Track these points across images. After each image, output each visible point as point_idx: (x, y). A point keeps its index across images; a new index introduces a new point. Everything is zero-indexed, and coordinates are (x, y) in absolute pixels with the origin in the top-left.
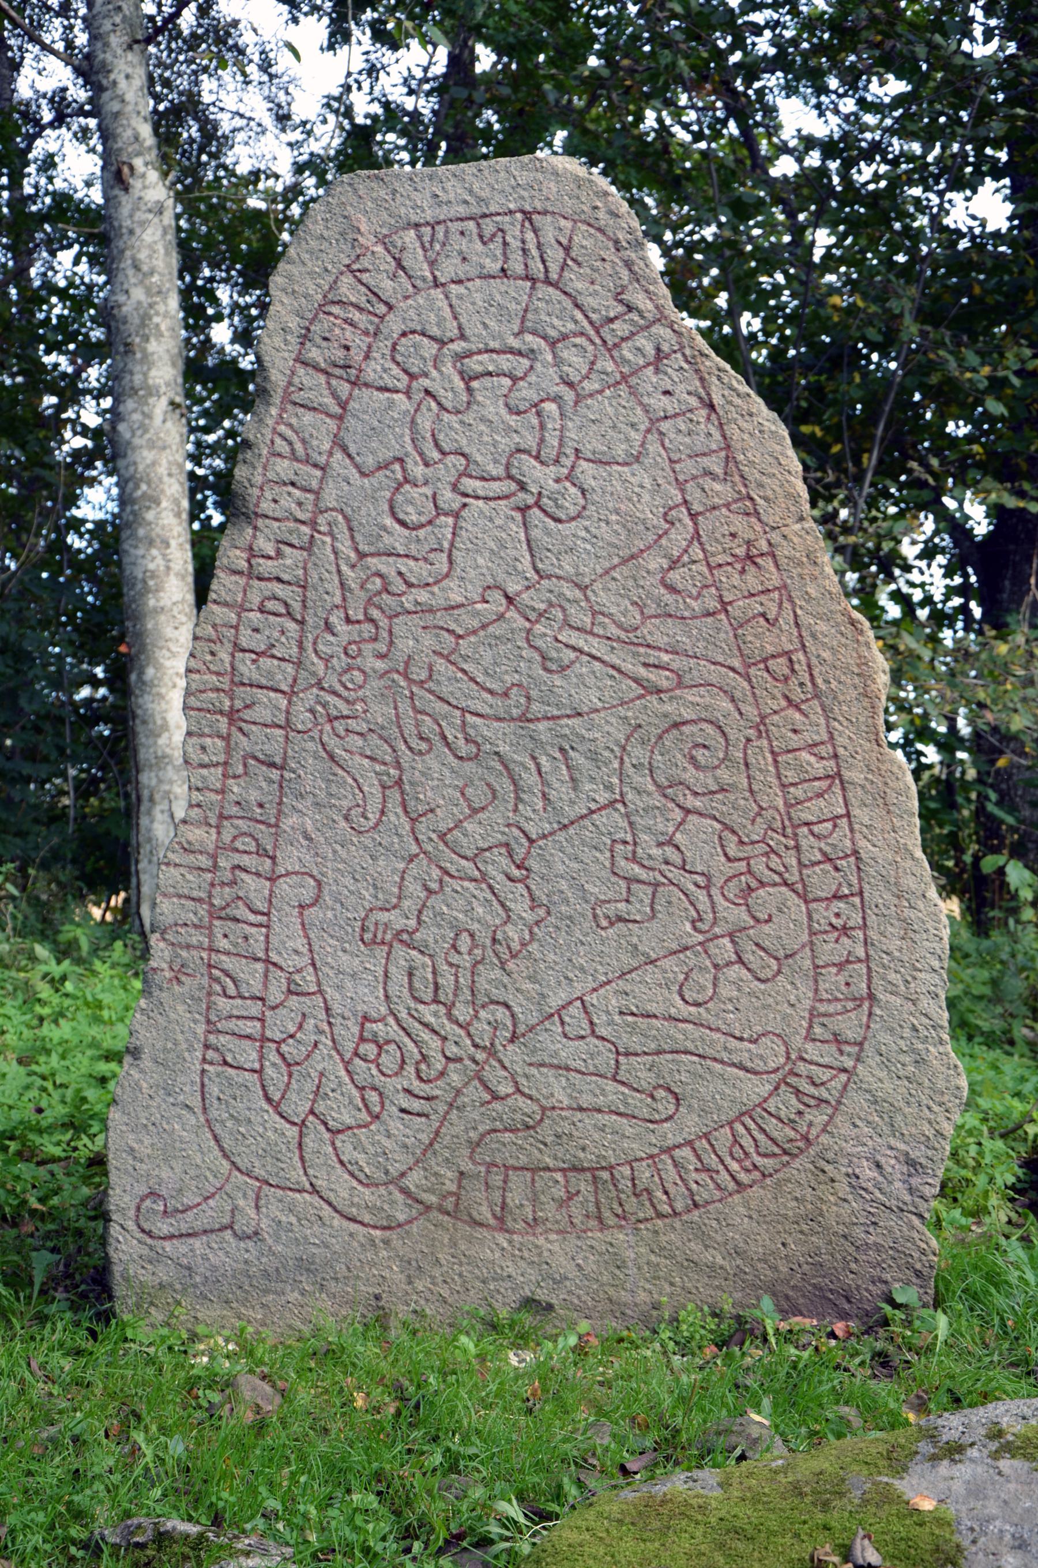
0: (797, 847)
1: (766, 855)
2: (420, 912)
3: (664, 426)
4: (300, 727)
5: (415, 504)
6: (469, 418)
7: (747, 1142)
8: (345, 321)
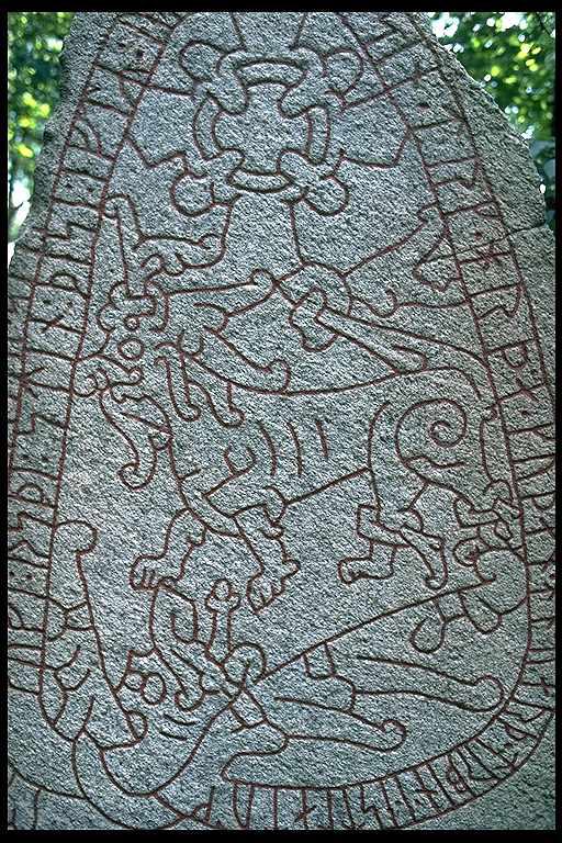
0: (521, 516)
1: (495, 522)
2: (184, 561)
3: (421, 134)
4: (83, 391)
5: (193, 192)
6: (247, 117)
7: (462, 769)
8: (140, 30)
